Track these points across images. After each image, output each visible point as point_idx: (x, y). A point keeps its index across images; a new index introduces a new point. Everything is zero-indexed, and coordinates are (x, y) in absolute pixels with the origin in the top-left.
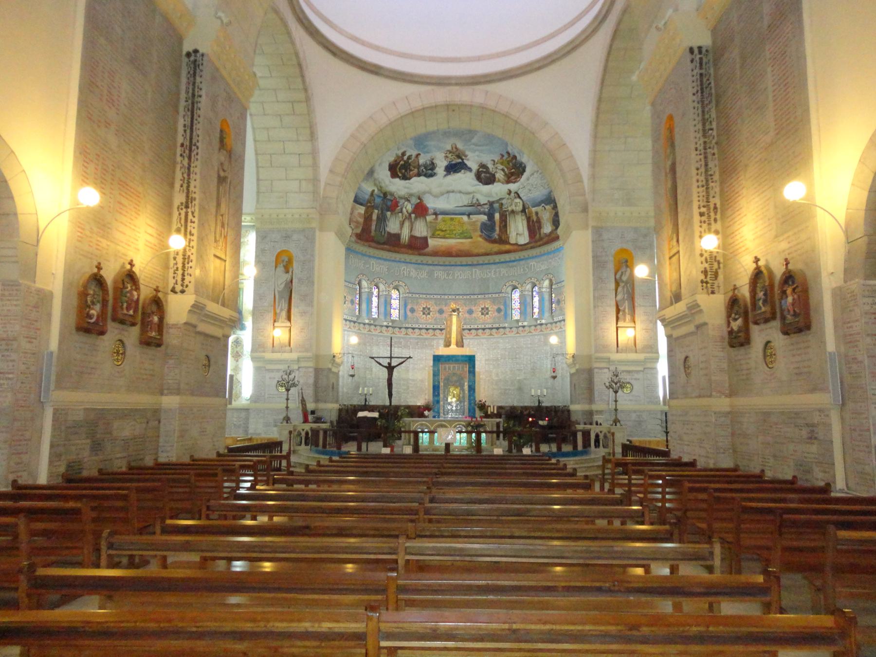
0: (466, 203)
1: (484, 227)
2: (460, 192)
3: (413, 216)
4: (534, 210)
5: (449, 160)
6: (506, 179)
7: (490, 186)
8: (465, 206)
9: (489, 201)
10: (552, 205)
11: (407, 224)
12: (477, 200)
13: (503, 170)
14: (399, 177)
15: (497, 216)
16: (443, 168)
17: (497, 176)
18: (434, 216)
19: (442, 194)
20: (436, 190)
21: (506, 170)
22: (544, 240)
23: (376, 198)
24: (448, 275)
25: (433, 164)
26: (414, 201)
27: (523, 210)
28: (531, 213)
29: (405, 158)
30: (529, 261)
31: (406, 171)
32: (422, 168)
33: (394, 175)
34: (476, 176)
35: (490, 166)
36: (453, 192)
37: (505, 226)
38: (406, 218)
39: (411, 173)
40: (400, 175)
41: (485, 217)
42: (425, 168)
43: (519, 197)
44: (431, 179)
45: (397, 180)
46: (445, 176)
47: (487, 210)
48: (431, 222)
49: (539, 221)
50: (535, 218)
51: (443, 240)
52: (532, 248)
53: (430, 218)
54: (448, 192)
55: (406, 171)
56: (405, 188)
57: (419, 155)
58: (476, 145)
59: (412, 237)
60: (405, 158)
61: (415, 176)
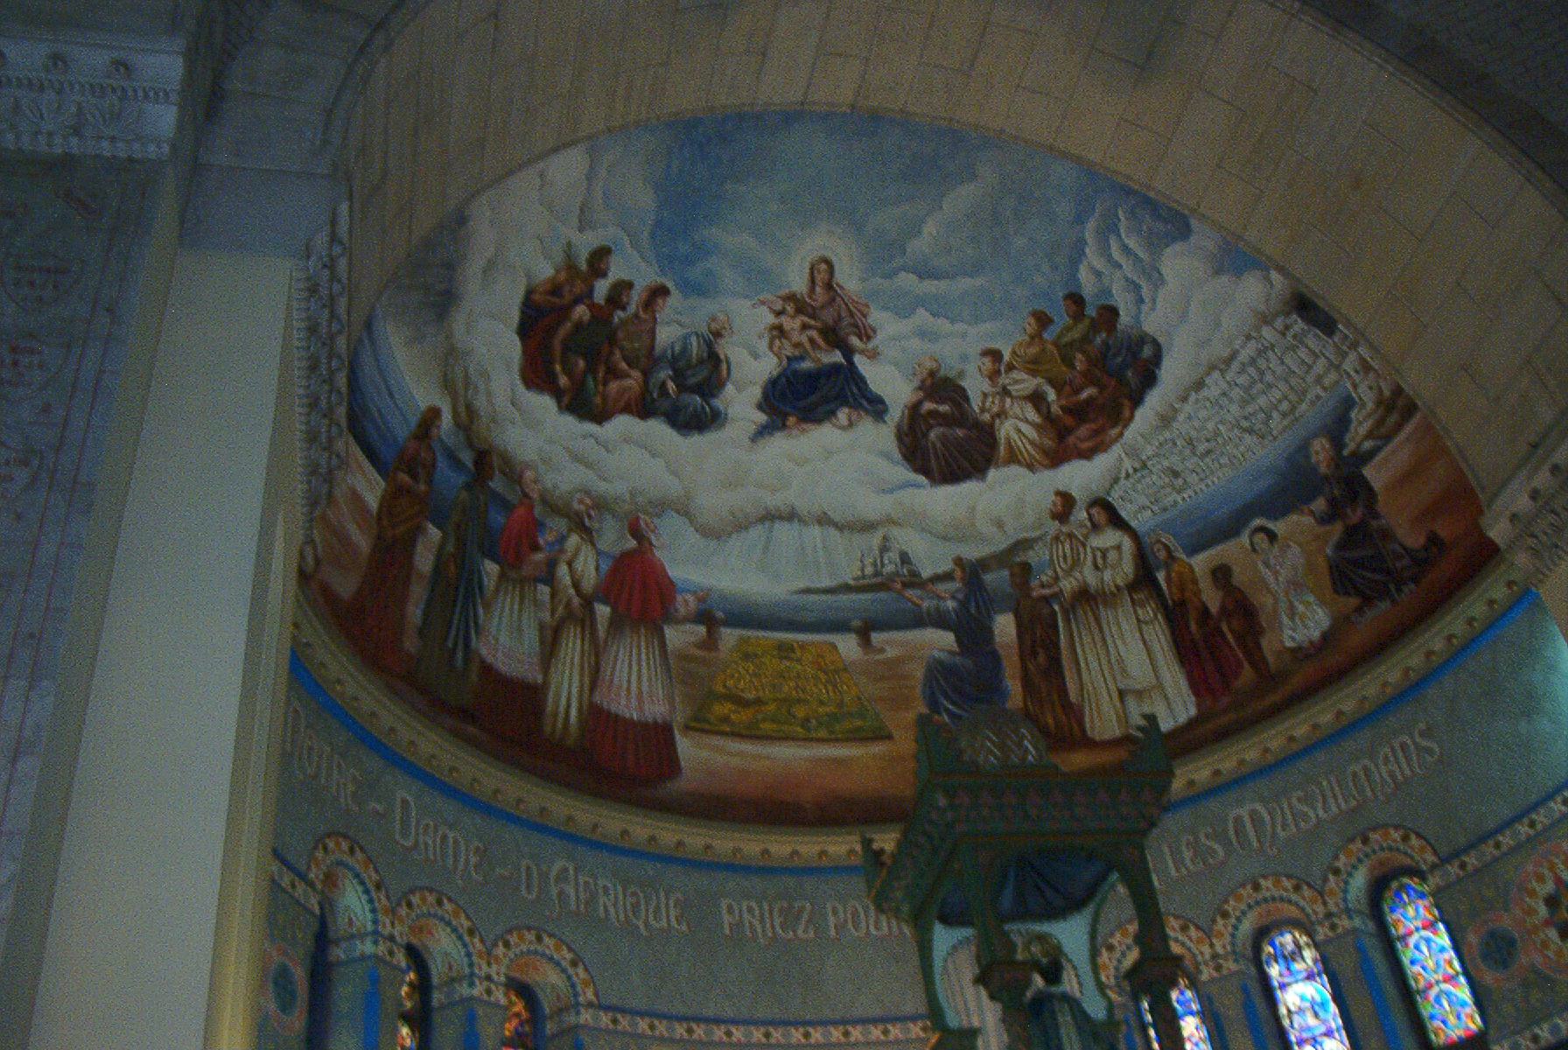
0: (849, 574)
1: (941, 676)
2: (824, 520)
3: (603, 611)
4: (1201, 562)
5: (789, 351)
6: (1048, 443)
7: (969, 487)
8: (846, 588)
9: (959, 561)
10: (1320, 504)
11: (572, 647)
12: (905, 558)
13: (1036, 399)
14: (557, 393)
15: (1005, 627)
16: (756, 392)
17: (1005, 430)
18: (702, 629)
19: (741, 525)
20: (713, 502)
21: (1052, 395)
22: (1296, 682)
23: (442, 463)
24: (791, 918)
25: (713, 359)
26: (613, 538)
27: (1144, 578)
28: (1186, 582)
29: (602, 288)
30: (1213, 804)
31: (591, 369)
32: (664, 374)
33: (537, 374)
34: (900, 436)
35: (976, 386)
36: (791, 516)
37: (1054, 668)
38: (570, 616)
39: (614, 386)
40: (563, 381)
41: (947, 639)
42: (678, 376)
43: (1117, 521)
44: (697, 440)
45: (544, 404)
46: (763, 432)
47: (951, 604)
48: (684, 657)
49: (1243, 610)
50: (1212, 598)
51: (748, 747)
52: (1223, 735)
53: (678, 636)
54: (770, 517)
55: (591, 369)
56: (577, 458)
57: (660, 292)
58: (925, 273)
59: (597, 717)
60: (602, 288)
61: (627, 409)
